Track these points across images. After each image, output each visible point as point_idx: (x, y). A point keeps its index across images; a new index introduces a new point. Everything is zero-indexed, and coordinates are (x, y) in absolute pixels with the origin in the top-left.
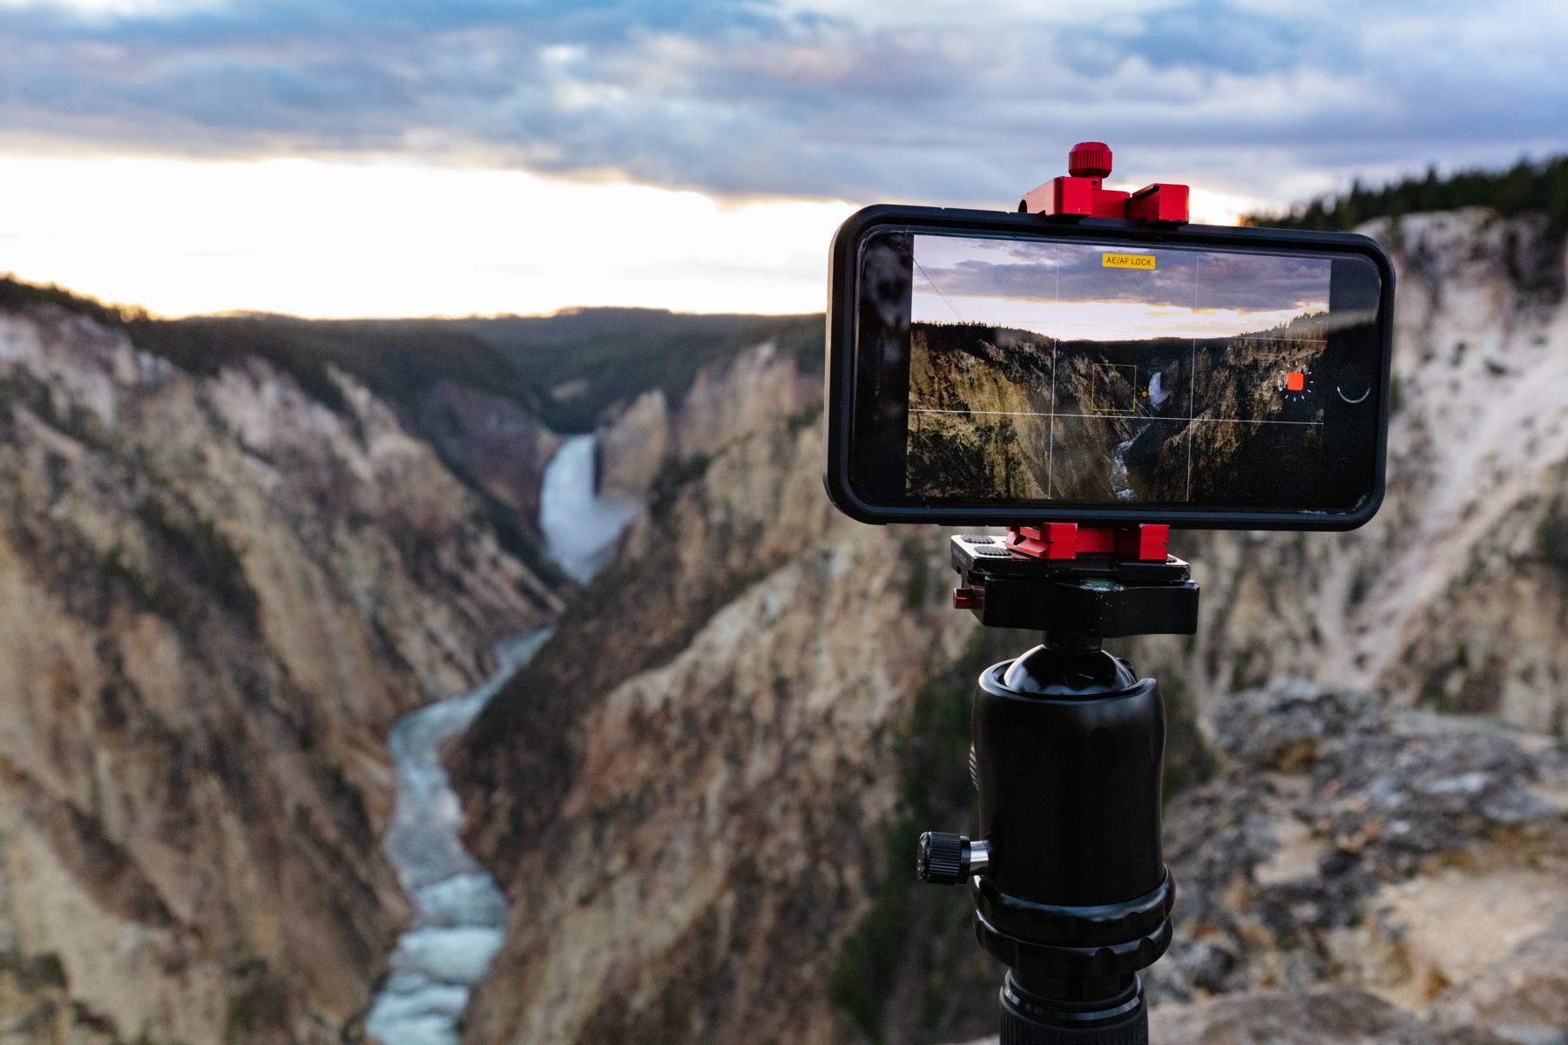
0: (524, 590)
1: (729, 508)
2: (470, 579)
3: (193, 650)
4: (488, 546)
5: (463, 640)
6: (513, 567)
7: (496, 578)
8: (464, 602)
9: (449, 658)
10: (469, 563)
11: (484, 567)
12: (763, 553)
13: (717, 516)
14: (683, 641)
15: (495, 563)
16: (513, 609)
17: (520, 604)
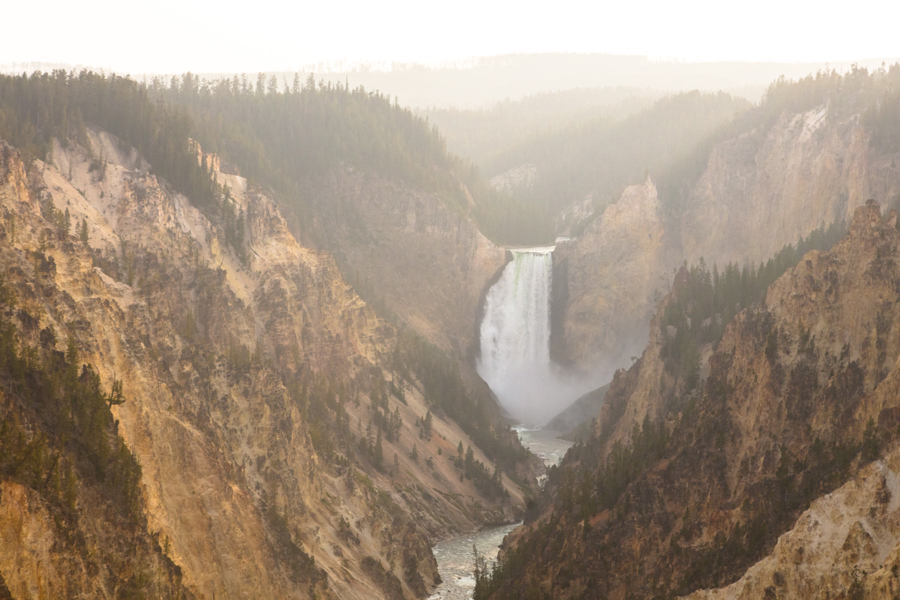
0: (467, 468)
1: (810, 352)
2: (389, 450)
3: (67, 537)
4: (416, 403)
5: (388, 539)
6: (448, 433)
7: (428, 450)
8: (382, 484)
9: (369, 564)
10: (388, 428)
11: (408, 434)
12: (868, 414)
13: (790, 359)
14: (758, 543)
15: (424, 429)
16: (452, 496)
17: (462, 488)
